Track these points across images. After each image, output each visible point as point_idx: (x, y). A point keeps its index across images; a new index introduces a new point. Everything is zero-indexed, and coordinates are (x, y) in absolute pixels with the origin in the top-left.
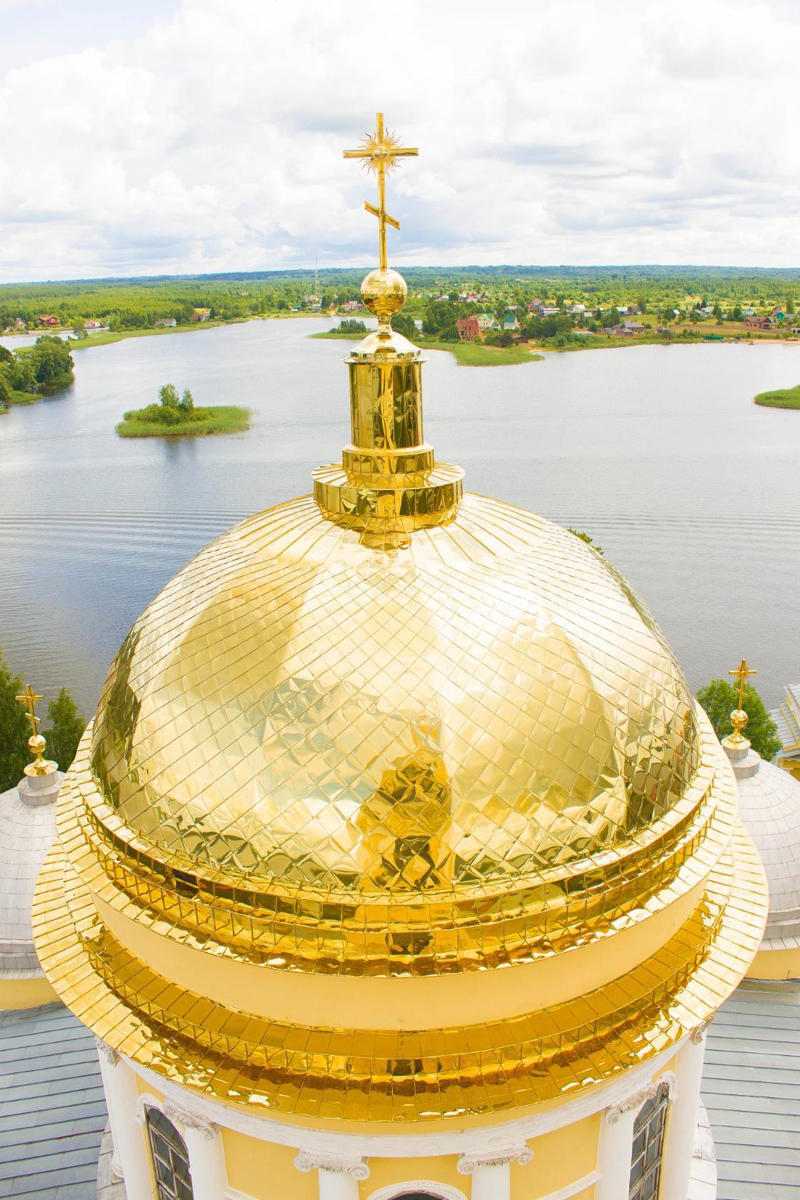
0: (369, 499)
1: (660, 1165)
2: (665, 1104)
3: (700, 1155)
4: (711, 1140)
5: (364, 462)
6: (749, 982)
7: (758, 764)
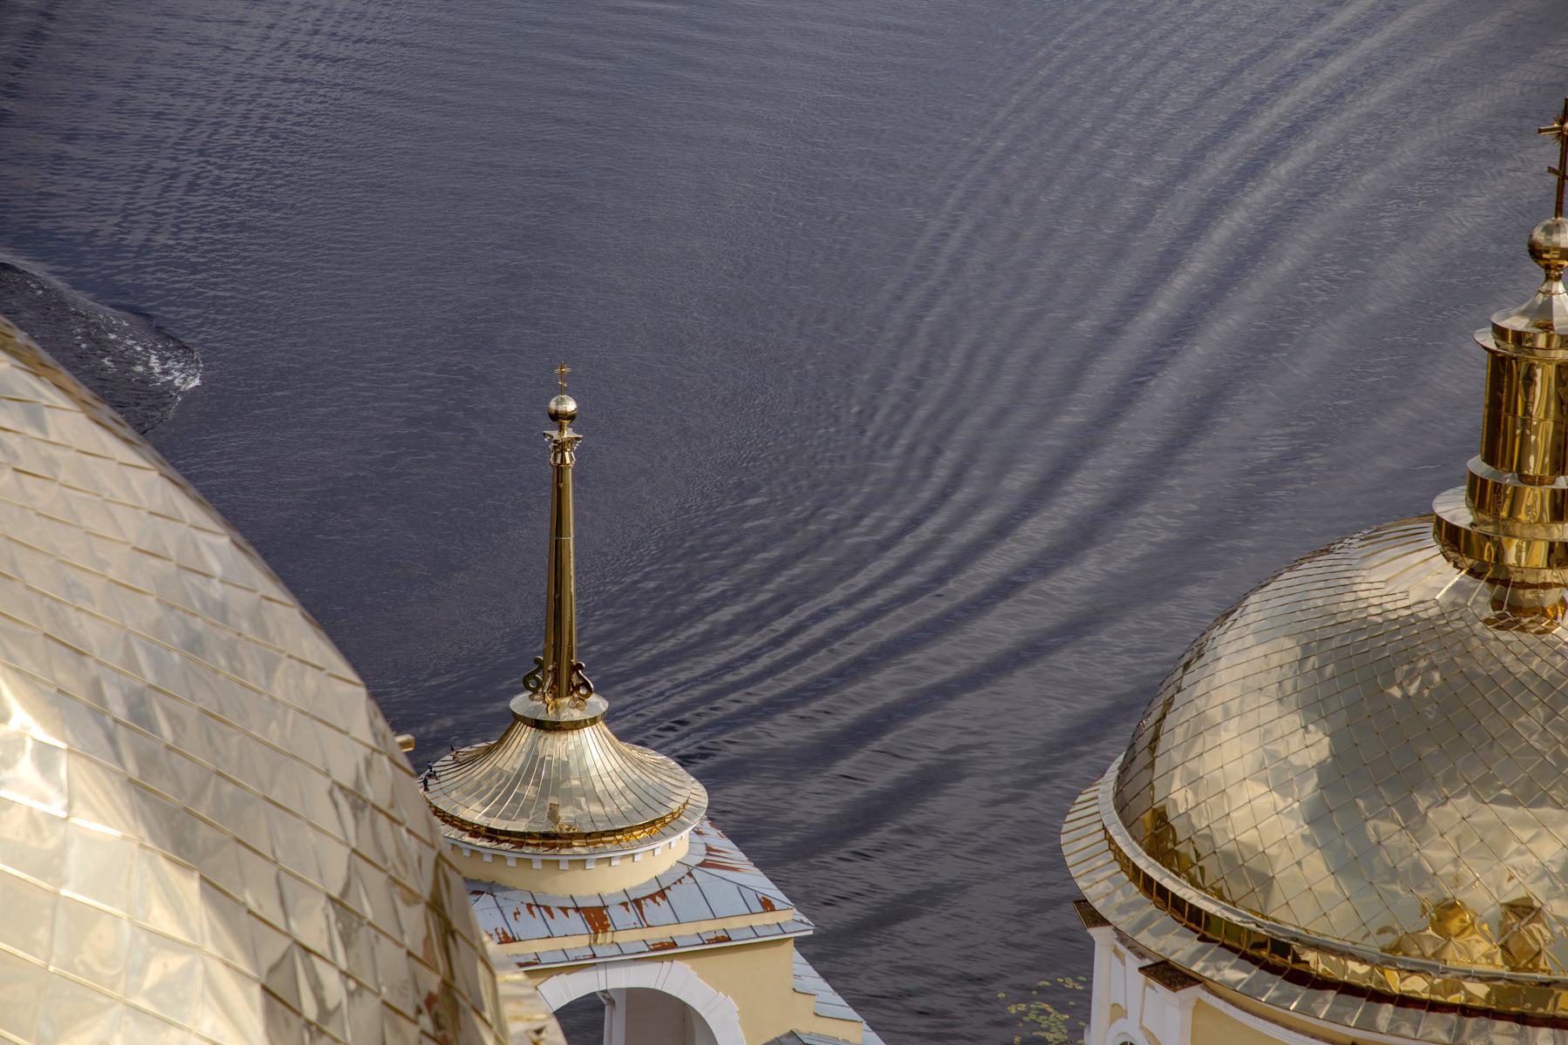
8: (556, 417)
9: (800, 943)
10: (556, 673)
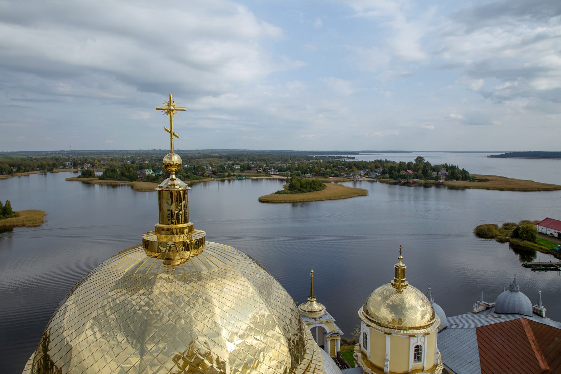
0: (172, 246)
5: (166, 231)
8: (312, 272)
9: (334, 322)
10: (312, 296)
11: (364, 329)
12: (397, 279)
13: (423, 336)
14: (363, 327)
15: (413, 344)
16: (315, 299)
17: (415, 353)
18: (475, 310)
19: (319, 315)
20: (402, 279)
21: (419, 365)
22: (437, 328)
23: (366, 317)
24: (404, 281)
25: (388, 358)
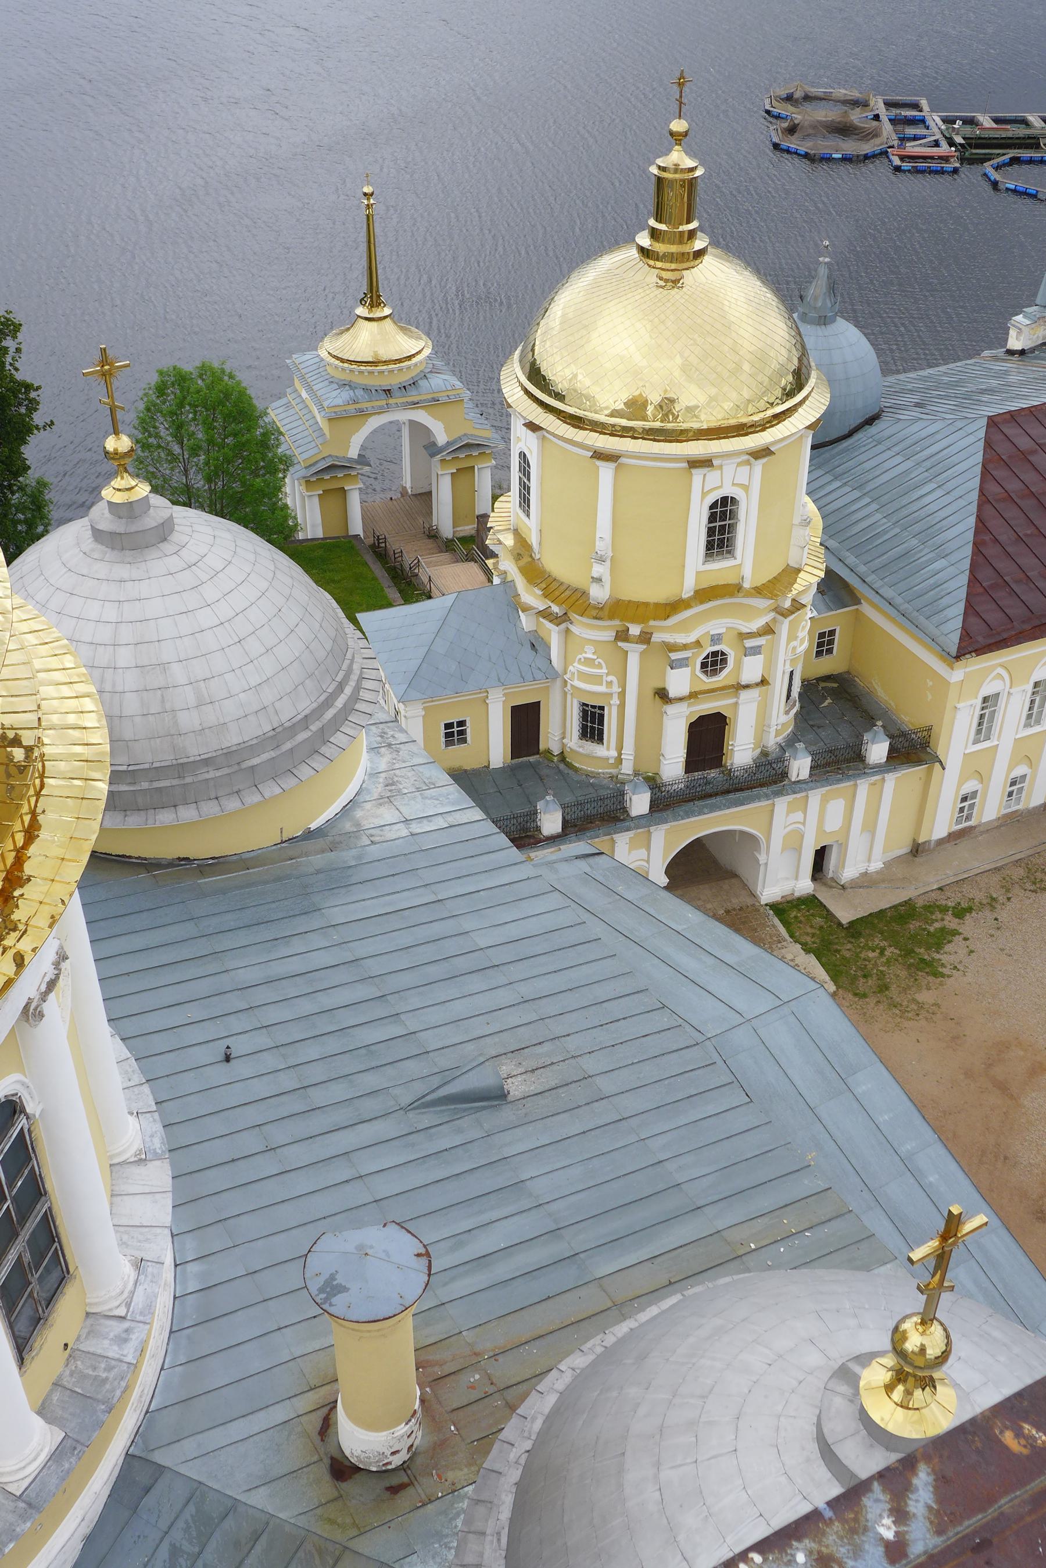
1: (50, 1208)
2: (22, 1123)
3: (143, 1156)
4: (158, 1127)
6: (223, 863)
7: (171, 517)
8: (365, 194)
10: (371, 297)
11: (519, 439)
12: (662, 227)
13: (748, 463)
14: (515, 430)
15: (704, 495)
16: (387, 311)
17: (709, 529)
18: (1015, 343)
19: (405, 378)
20: (681, 228)
21: (721, 568)
22: (808, 427)
23: (527, 392)
24: (692, 234)
25: (603, 543)
